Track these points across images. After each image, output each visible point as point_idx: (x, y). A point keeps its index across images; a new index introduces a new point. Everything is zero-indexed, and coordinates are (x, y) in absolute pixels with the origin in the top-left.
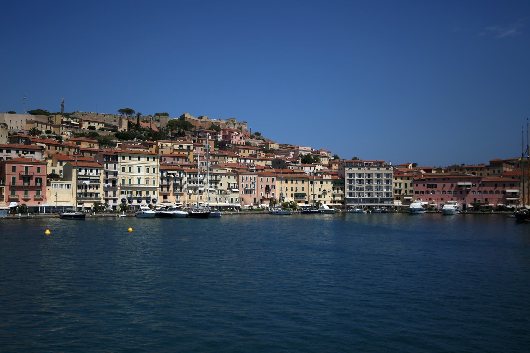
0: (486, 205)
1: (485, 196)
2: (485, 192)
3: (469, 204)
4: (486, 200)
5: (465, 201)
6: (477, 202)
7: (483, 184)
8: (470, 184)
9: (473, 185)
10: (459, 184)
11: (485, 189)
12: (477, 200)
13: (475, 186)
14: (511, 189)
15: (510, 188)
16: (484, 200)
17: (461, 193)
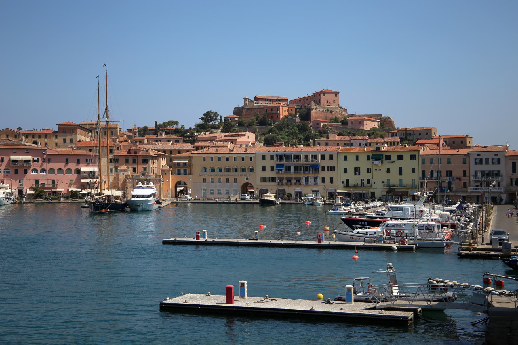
0: (53, 190)
1: (52, 177)
2: (52, 171)
3: (28, 190)
4: (53, 182)
5: (22, 185)
6: (40, 186)
7: (48, 159)
8: (29, 158)
9: (34, 161)
10: (13, 158)
11: (51, 165)
12: (40, 183)
13: (37, 161)
14: (88, 166)
15: (86, 164)
16: (50, 183)
17: (16, 172)
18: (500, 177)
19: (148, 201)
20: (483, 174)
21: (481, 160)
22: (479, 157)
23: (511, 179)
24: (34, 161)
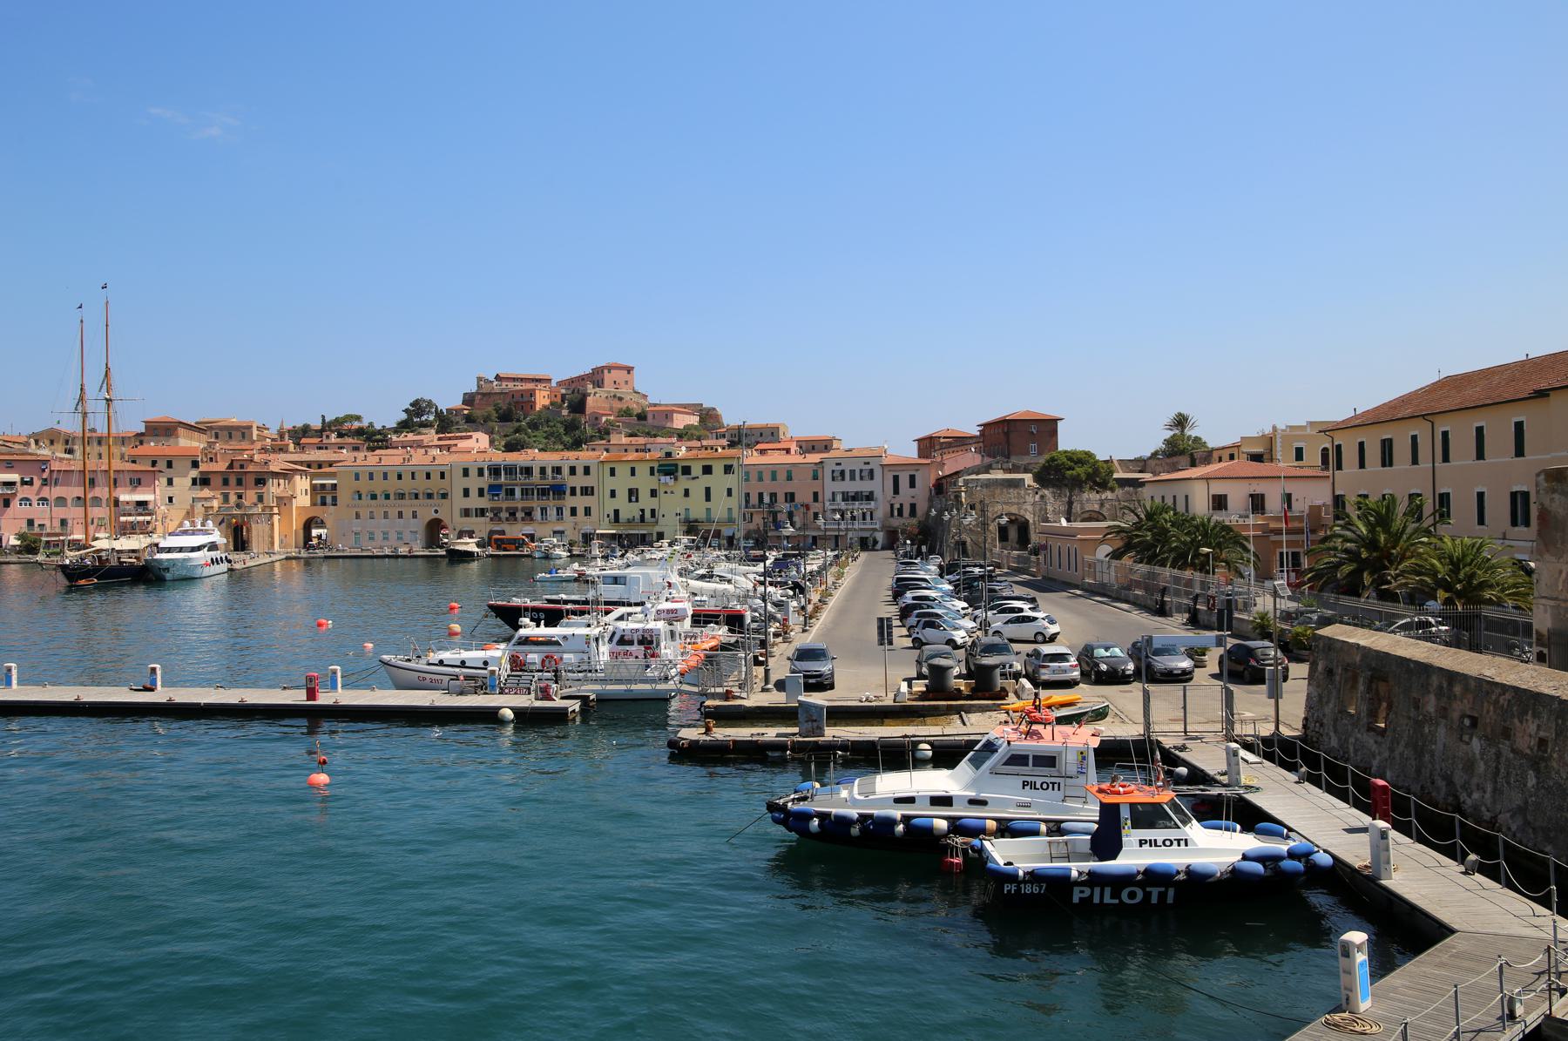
1: (60, 512)
2: (61, 501)
3: (12, 537)
4: (63, 522)
6: (37, 530)
11: (58, 491)
13: (31, 483)
16: (57, 523)
18: (872, 503)
19: (189, 559)
20: (846, 497)
21: (842, 473)
22: (839, 468)
23: (892, 506)
24: (24, 483)
